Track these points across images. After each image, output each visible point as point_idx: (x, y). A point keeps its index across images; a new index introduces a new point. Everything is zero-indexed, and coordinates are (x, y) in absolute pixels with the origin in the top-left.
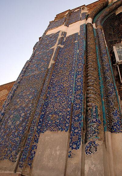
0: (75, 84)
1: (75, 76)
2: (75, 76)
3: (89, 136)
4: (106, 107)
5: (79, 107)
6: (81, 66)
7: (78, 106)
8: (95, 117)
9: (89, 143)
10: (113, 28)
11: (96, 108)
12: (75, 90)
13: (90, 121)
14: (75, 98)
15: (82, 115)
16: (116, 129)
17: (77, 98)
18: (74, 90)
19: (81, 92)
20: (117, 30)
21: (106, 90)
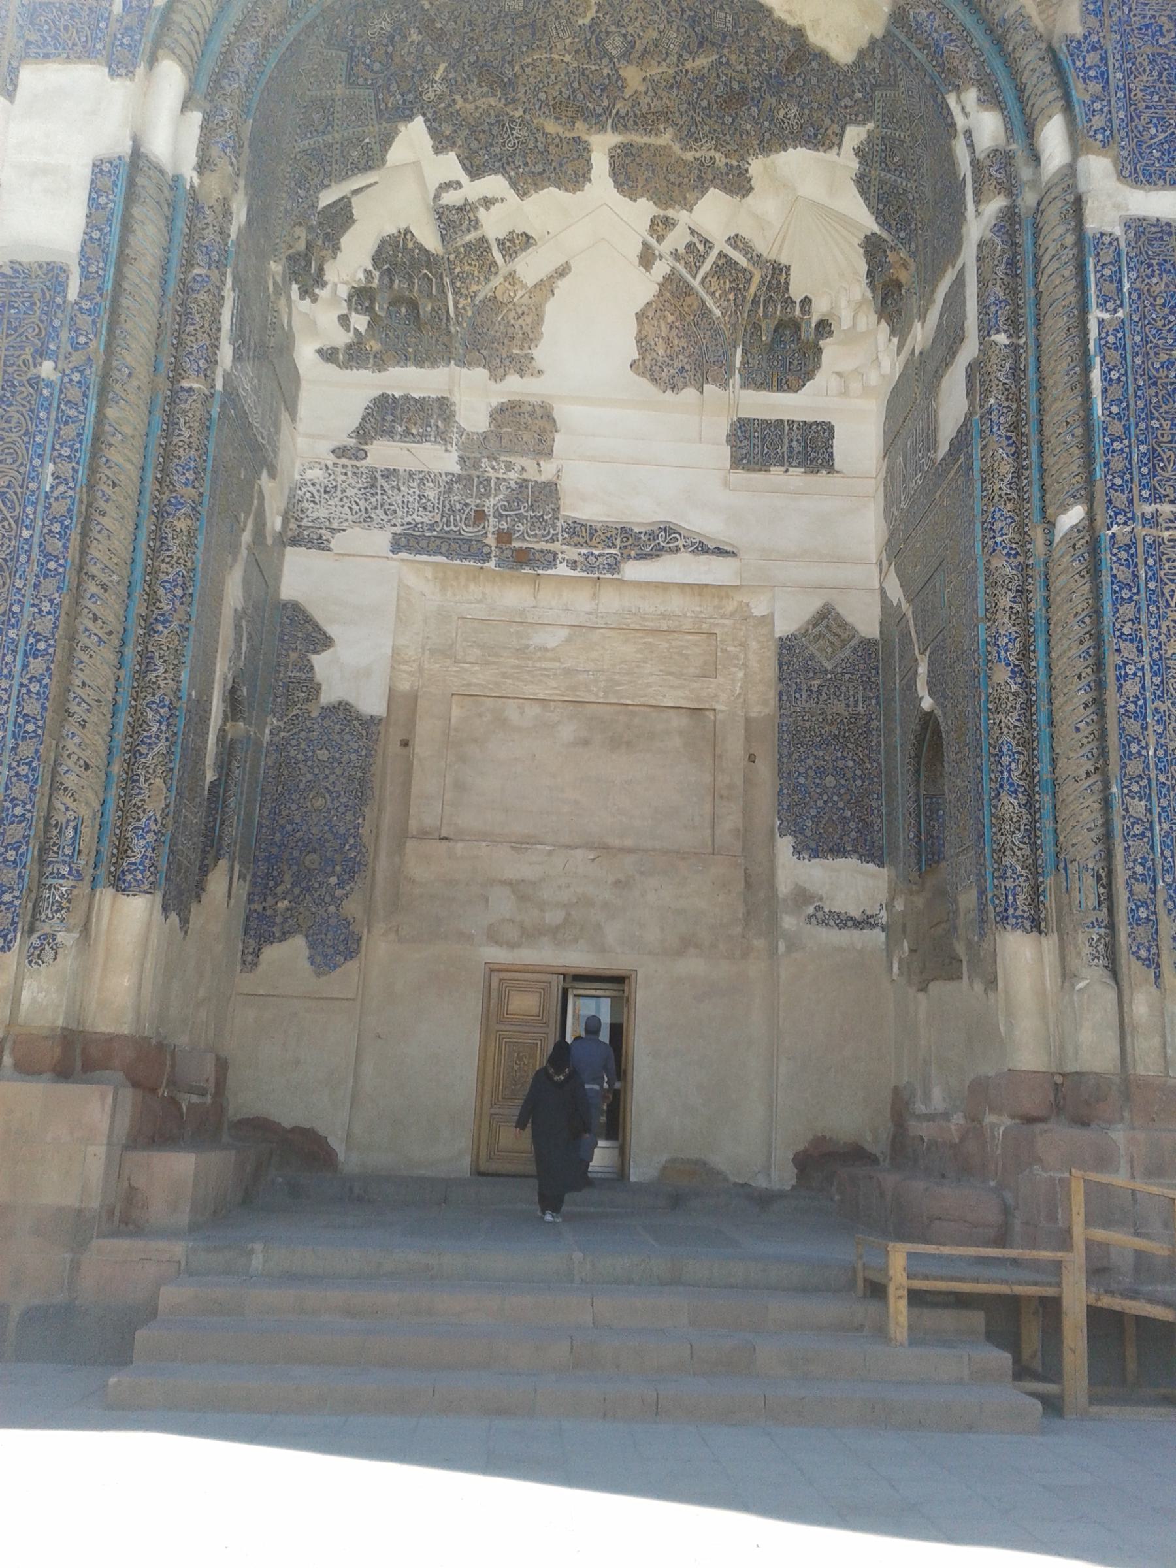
0: (18, 704)
1: (19, 658)
2: (19, 658)
3: (43, 917)
4: (120, 797)
5: (23, 815)
6: (51, 601)
7: (18, 811)
8: (67, 859)
9: (39, 938)
10: (351, 59)
11: (75, 829)
12: (14, 736)
13: (50, 869)
14: (13, 773)
15: (31, 847)
16: (130, 883)
17: (17, 774)
18: (9, 734)
19: (37, 751)
20: (377, 66)
21: (137, 725)
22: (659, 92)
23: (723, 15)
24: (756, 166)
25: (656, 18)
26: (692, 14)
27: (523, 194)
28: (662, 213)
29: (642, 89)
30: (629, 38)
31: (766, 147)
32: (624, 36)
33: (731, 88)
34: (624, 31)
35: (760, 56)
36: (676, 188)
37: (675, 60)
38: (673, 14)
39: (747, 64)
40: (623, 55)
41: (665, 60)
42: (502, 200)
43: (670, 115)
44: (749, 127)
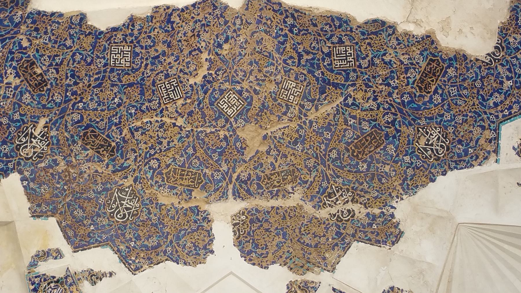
22: (283, 149)
23: (342, 49)
24: (402, 209)
25: (272, 69)
26: (310, 57)
27: (136, 270)
28: (299, 278)
29: (264, 149)
30: (245, 94)
31: (410, 187)
32: (240, 93)
33: (362, 129)
34: (238, 88)
35: (389, 85)
36: (313, 249)
37: (296, 112)
38: (289, 62)
39: (375, 99)
40: (240, 114)
41: (285, 114)
42: (111, 274)
43: (297, 173)
44: (387, 168)
